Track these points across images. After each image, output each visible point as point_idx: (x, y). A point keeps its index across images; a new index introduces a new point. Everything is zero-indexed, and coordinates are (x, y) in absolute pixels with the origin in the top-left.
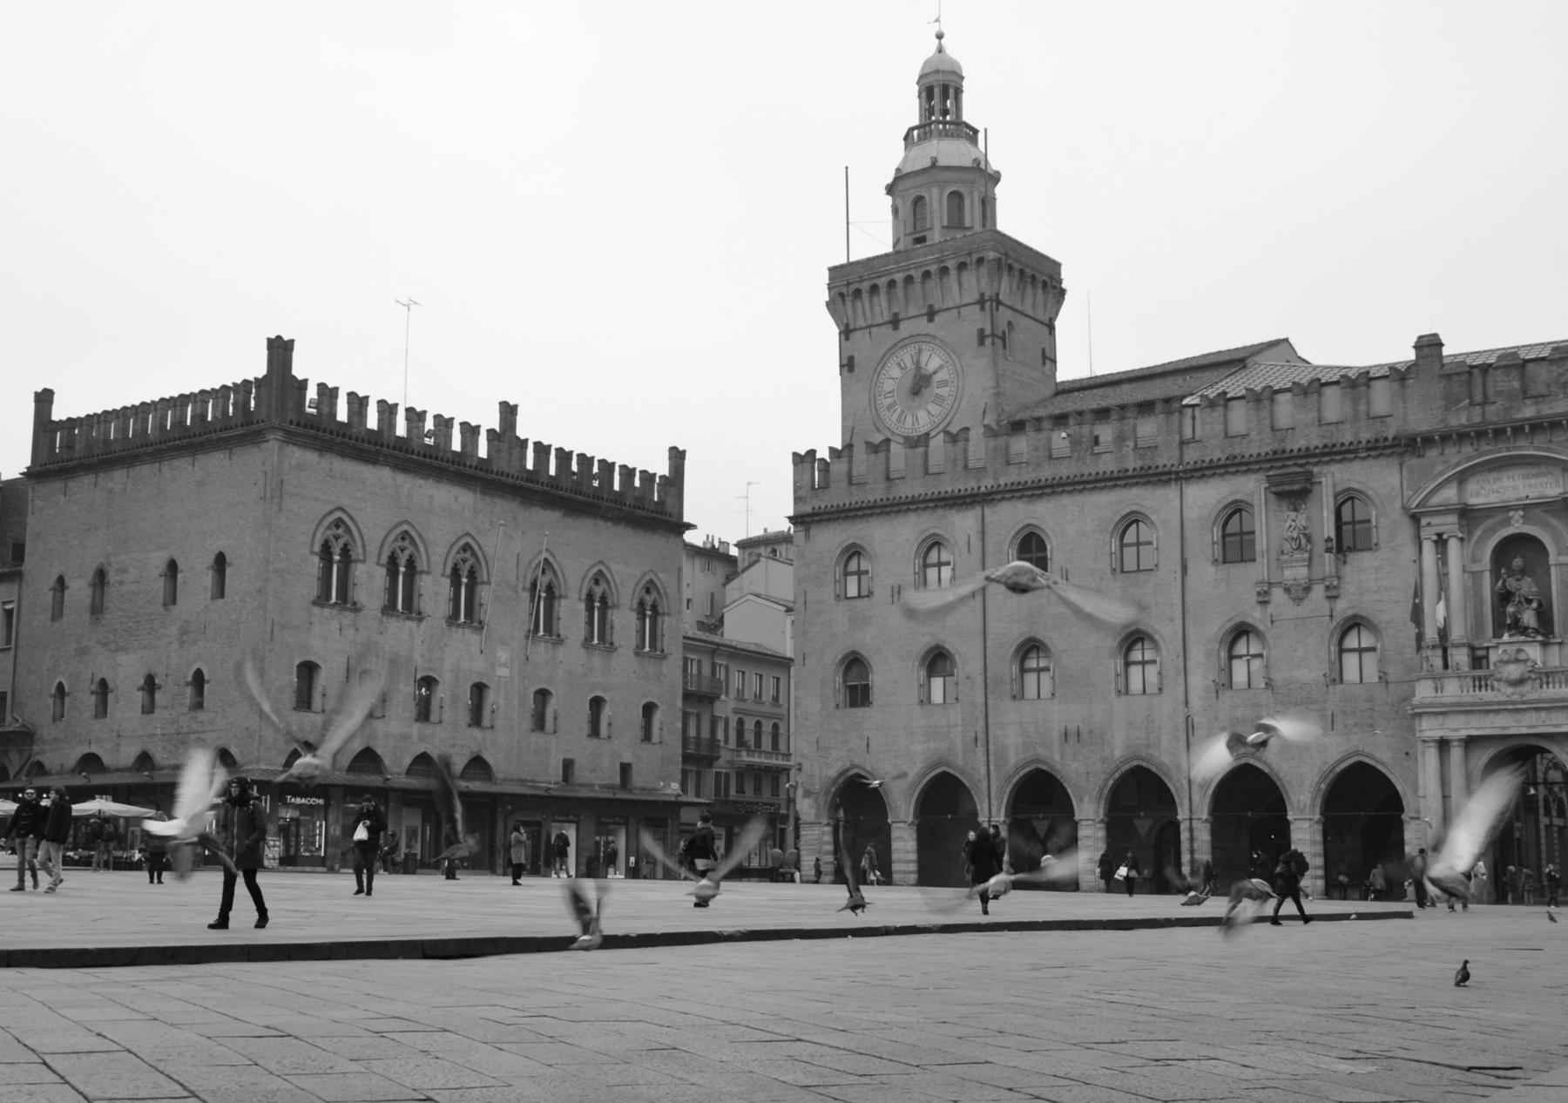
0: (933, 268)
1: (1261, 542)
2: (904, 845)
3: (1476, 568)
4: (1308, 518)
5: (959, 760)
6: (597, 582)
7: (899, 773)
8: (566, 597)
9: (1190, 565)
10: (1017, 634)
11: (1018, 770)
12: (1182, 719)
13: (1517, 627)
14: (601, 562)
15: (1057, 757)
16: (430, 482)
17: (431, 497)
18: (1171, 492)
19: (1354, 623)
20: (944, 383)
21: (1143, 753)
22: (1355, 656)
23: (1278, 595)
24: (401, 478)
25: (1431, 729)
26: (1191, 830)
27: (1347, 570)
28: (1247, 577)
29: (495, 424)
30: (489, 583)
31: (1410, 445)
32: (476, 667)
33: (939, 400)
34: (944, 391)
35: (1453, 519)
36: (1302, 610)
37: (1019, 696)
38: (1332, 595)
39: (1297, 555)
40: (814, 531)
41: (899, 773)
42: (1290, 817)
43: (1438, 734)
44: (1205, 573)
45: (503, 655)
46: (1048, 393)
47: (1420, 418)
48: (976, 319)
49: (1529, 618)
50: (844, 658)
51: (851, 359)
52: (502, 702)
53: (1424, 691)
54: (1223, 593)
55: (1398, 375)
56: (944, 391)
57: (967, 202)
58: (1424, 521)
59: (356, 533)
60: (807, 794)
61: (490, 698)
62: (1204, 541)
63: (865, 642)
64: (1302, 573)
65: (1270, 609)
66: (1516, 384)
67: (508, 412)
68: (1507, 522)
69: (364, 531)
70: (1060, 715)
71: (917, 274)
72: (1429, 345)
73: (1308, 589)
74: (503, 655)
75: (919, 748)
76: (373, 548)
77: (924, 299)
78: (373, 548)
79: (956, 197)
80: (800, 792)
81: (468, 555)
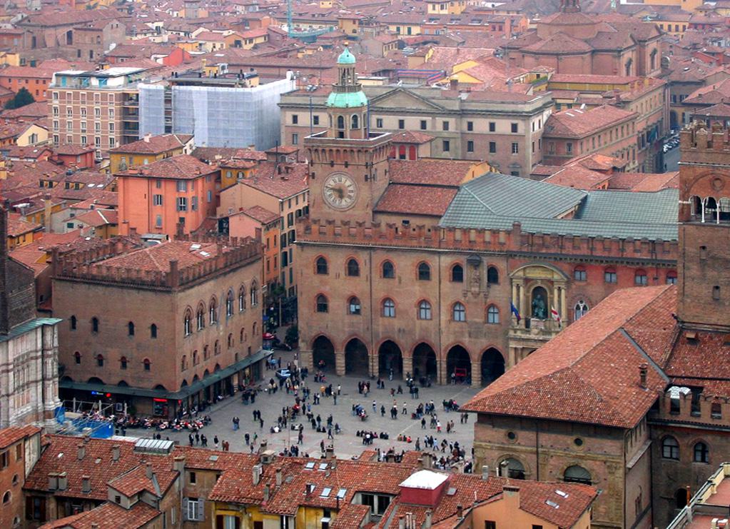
0: (348, 149)
1: (465, 278)
2: (341, 361)
3: (528, 294)
4: (480, 273)
5: (362, 335)
7: (340, 339)
9: (442, 280)
10: (382, 295)
11: (383, 338)
12: (437, 330)
13: (537, 316)
15: (396, 338)
18: (436, 258)
19: (493, 305)
20: (352, 191)
21: (426, 338)
22: (492, 315)
23: (469, 294)
25: (513, 345)
26: (441, 364)
27: (491, 290)
28: (459, 288)
31: (510, 255)
33: (350, 197)
34: (352, 194)
35: (522, 281)
36: (476, 300)
37: (383, 315)
38: (486, 297)
39: (476, 284)
40: (305, 249)
41: (340, 339)
42: (471, 362)
43: (514, 346)
44: (447, 285)
46: (386, 186)
47: (514, 246)
48: (364, 172)
49: (541, 314)
50: (318, 295)
51: (313, 174)
53: (511, 333)
54: (452, 291)
55: (508, 233)
56: (352, 194)
57: (359, 119)
58: (514, 280)
60: (303, 341)
61: (220, 343)
62: (447, 274)
63: (326, 290)
64: (477, 289)
65: (467, 299)
66: (541, 242)
68: (536, 283)
70: (397, 324)
71: (342, 150)
72: (517, 226)
73: (479, 294)
75: (346, 329)
77: (344, 158)
78: (195, 312)
79: (355, 118)
80: (300, 340)
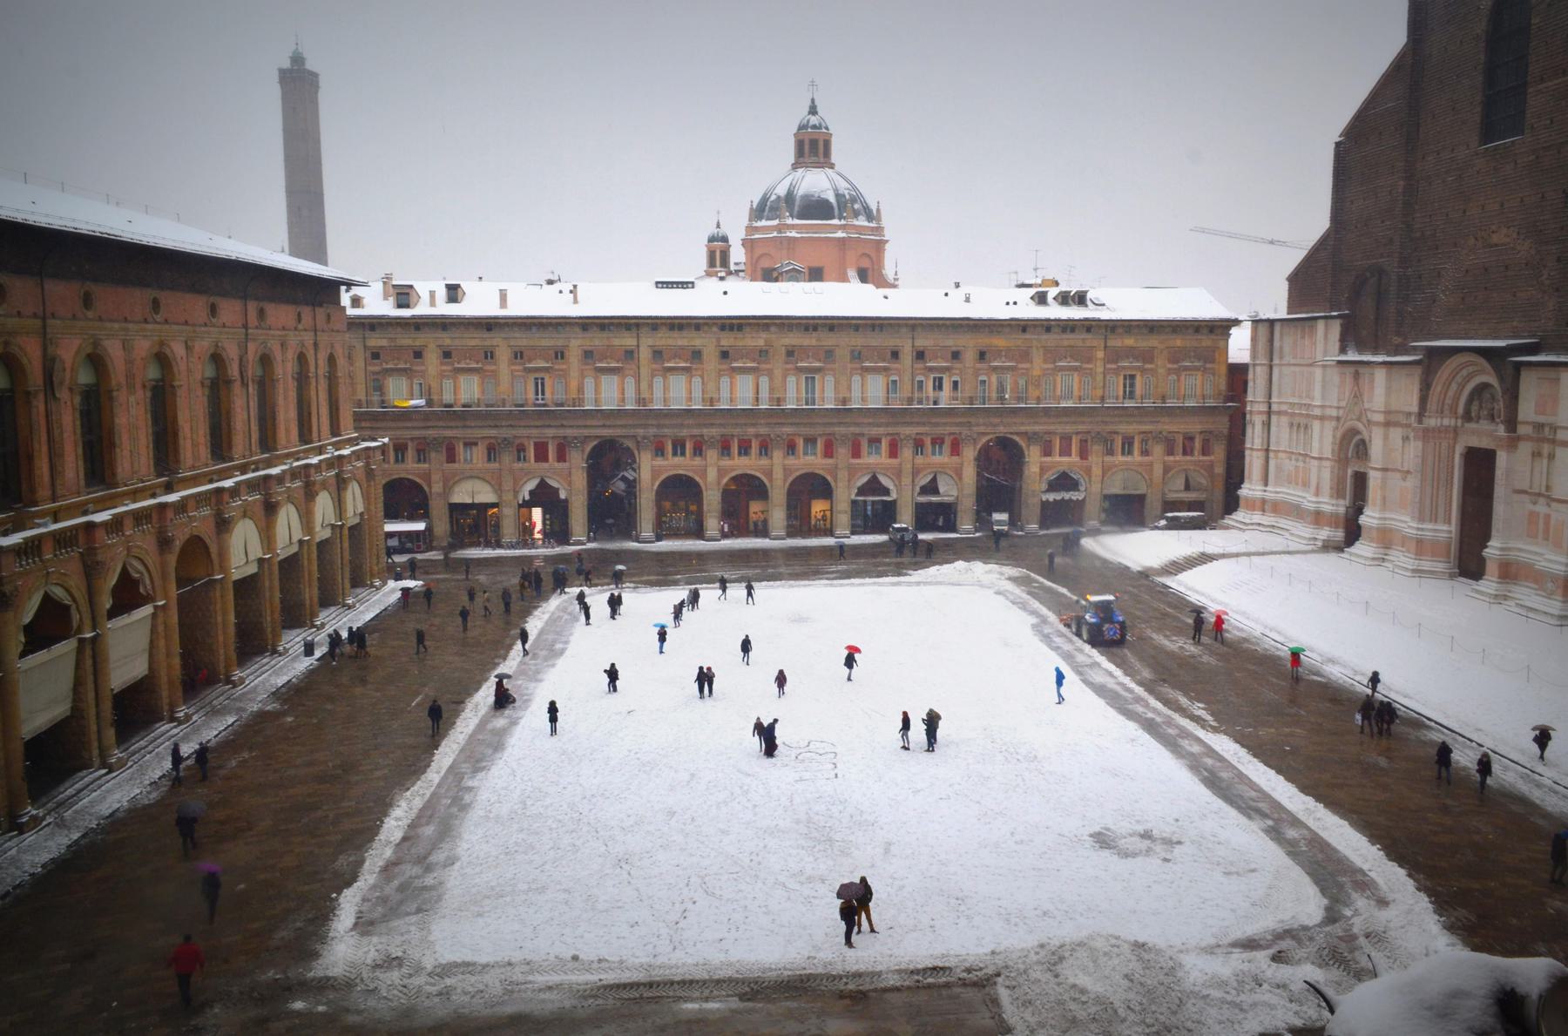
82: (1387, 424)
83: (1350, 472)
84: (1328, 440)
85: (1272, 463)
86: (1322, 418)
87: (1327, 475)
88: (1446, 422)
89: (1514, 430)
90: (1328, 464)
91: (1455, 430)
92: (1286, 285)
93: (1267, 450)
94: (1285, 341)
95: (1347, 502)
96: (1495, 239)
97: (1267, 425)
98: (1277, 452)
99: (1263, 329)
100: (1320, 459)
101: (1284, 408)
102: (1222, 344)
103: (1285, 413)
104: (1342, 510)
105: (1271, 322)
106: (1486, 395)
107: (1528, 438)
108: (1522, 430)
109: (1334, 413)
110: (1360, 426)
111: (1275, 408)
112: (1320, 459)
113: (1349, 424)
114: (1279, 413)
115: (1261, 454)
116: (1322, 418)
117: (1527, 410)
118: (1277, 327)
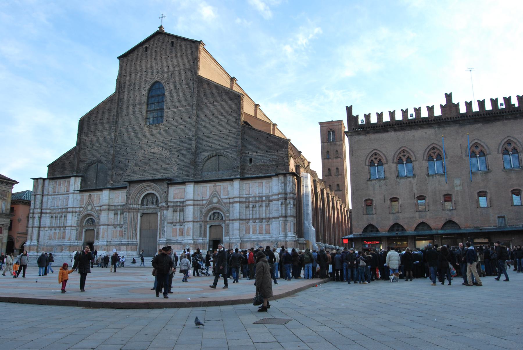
6: (510, 144)
8: (490, 154)
14: (508, 137)
16: (413, 131)
17: (414, 136)
24: (399, 133)
29: (444, 103)
30: (446, 158)
32: (445, 188)
45: (457, 182)
52: (460, 199)
59: (382, 156)
67: (449, 97)
69: (385, 154)
74: (457, 182)
76: (390, 158)
78: (390, 158)
81: (435, 150)
82: (109, 210)
83: (84, 230)
84: (75, 219)
85: (42, 233)
86: (72, 212)
87: (74, 233)
88: (135, 206)
89: (167, 204)
90: (74, 228)
91: (139, 209)
92: (47, 168)
93: (39, 227)
94: (50, 186)
95: (83, 241)
96: (152, 151)
97: (40, 218)
98: (44, 227)
99: (41, 181)
100: (71, 226)
101: (48, 211)
102: (10, 190)
103: (50, 213)
104: (81, 244)
105: (44, 179)
106: (150, 198)
107: (173, 207)
108: (169, 204)
109: (78, 210)
110: (92, 213)
111: (43, 211)
112: (71, 226)
113: (85, 213)
114: (46, 213)
115: (37, 229)
116: (72, 212)
117: (171, 199)
118: (47, 182)
